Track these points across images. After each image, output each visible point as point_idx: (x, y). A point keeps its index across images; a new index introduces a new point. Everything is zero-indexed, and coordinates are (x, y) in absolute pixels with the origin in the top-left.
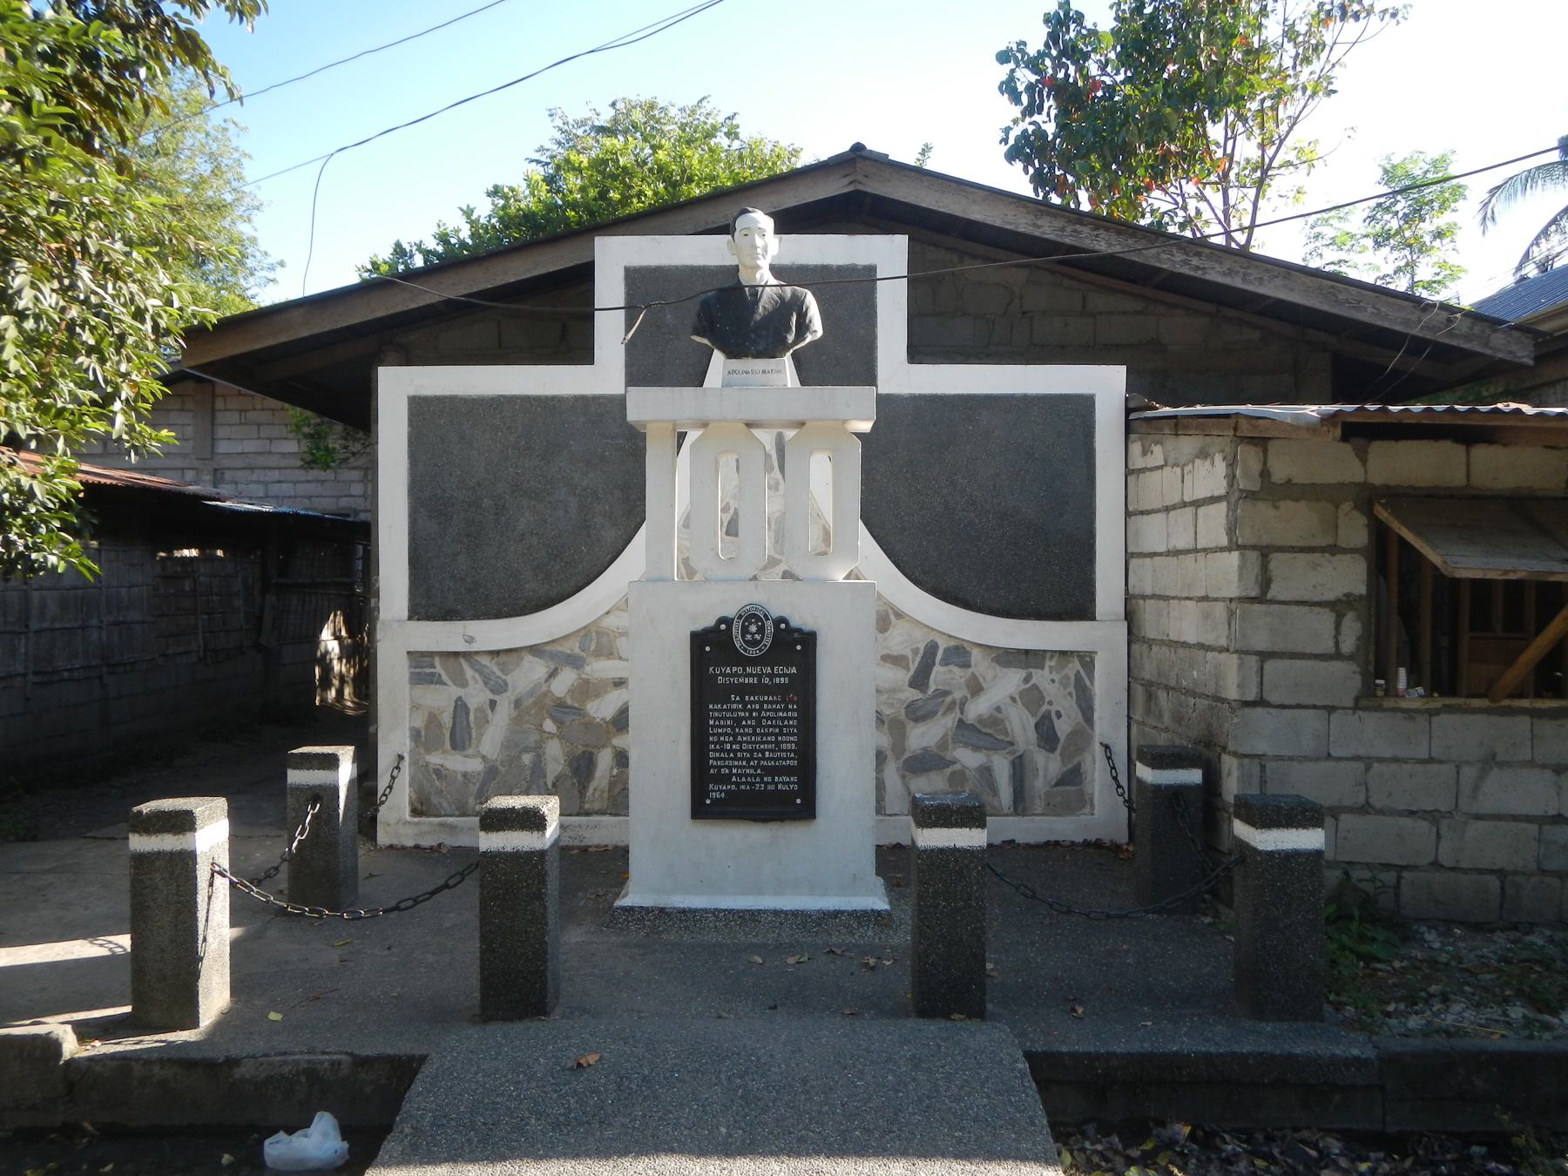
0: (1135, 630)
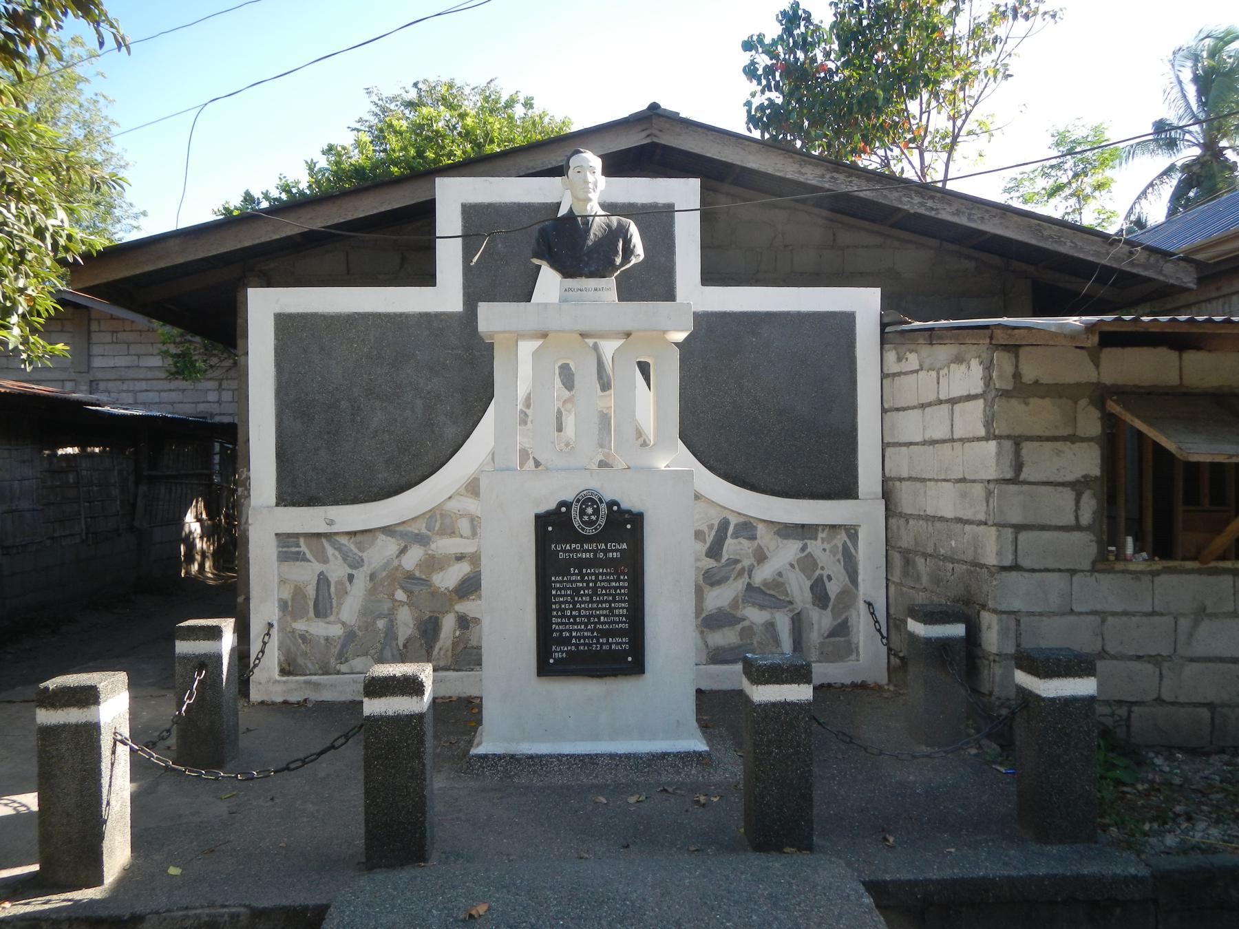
0: (892, 507)
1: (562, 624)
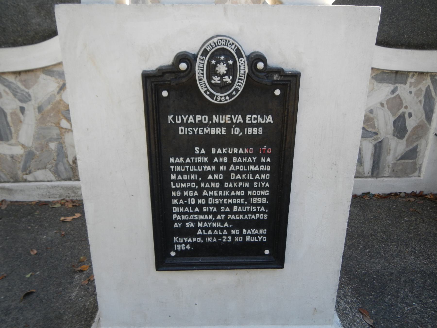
1: (184, 213)
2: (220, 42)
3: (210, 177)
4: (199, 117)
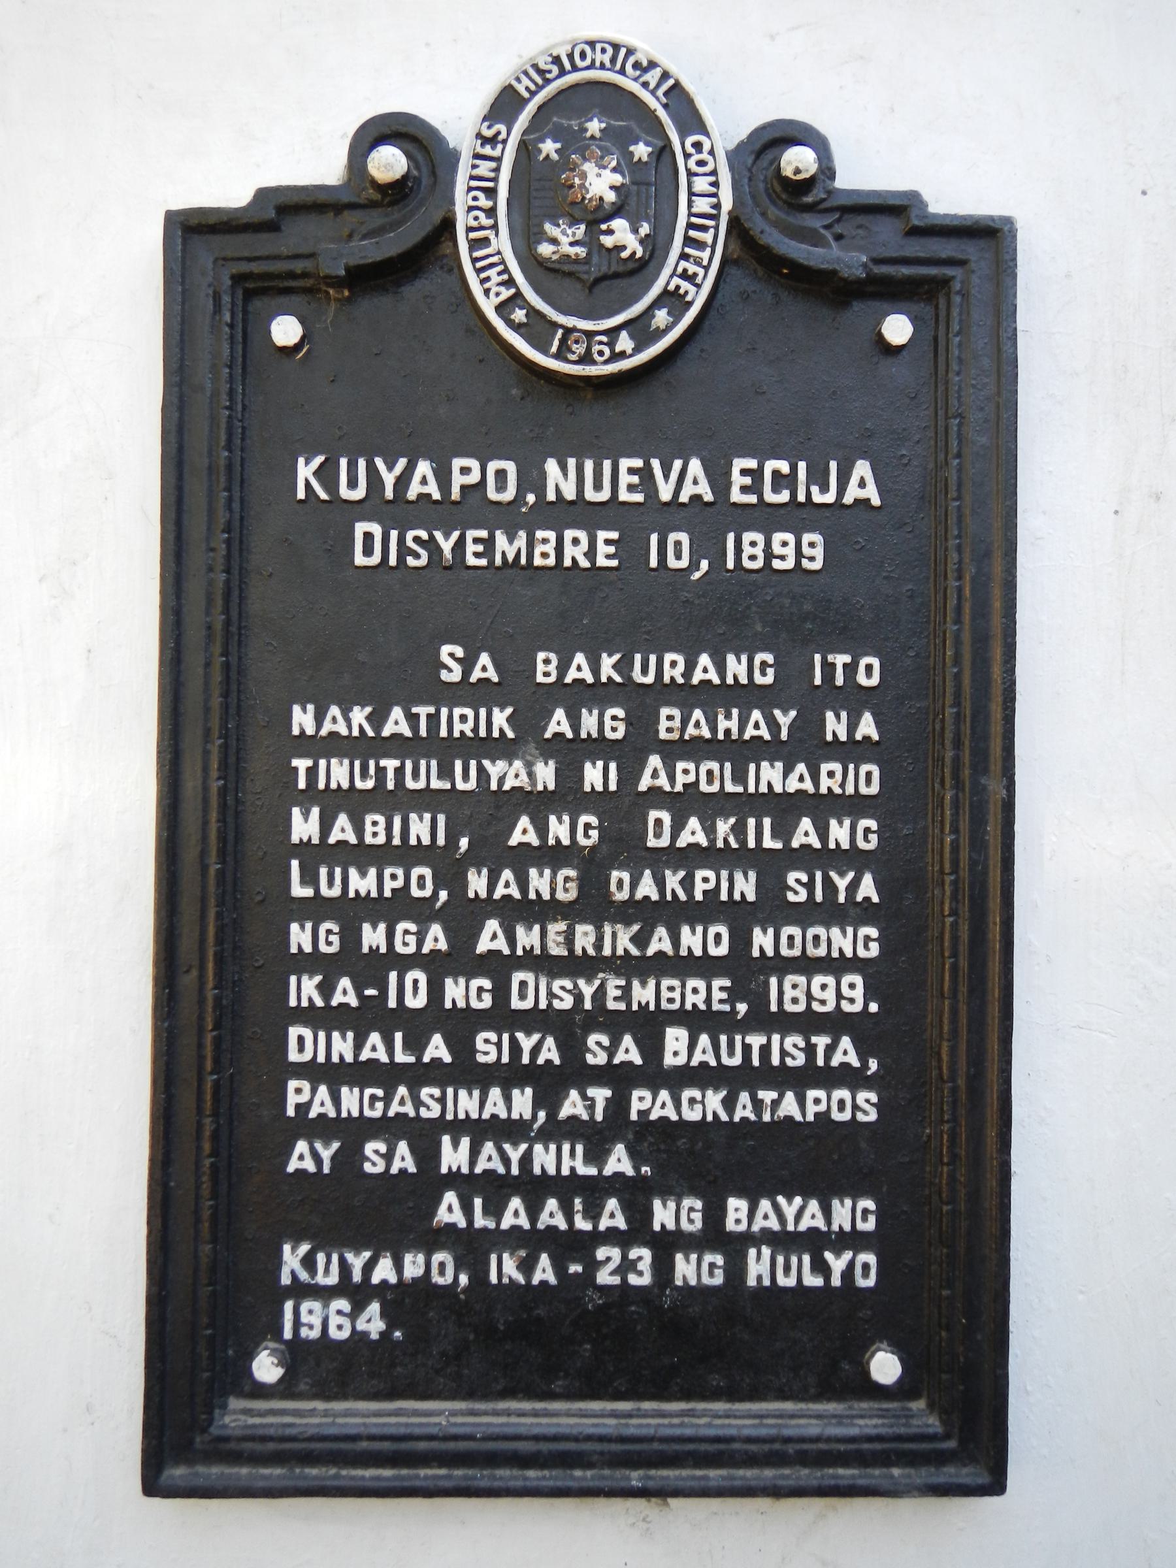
1: (361, 1073)
2: (583, 55)
3: (523, 832)
4: (465, 471)
